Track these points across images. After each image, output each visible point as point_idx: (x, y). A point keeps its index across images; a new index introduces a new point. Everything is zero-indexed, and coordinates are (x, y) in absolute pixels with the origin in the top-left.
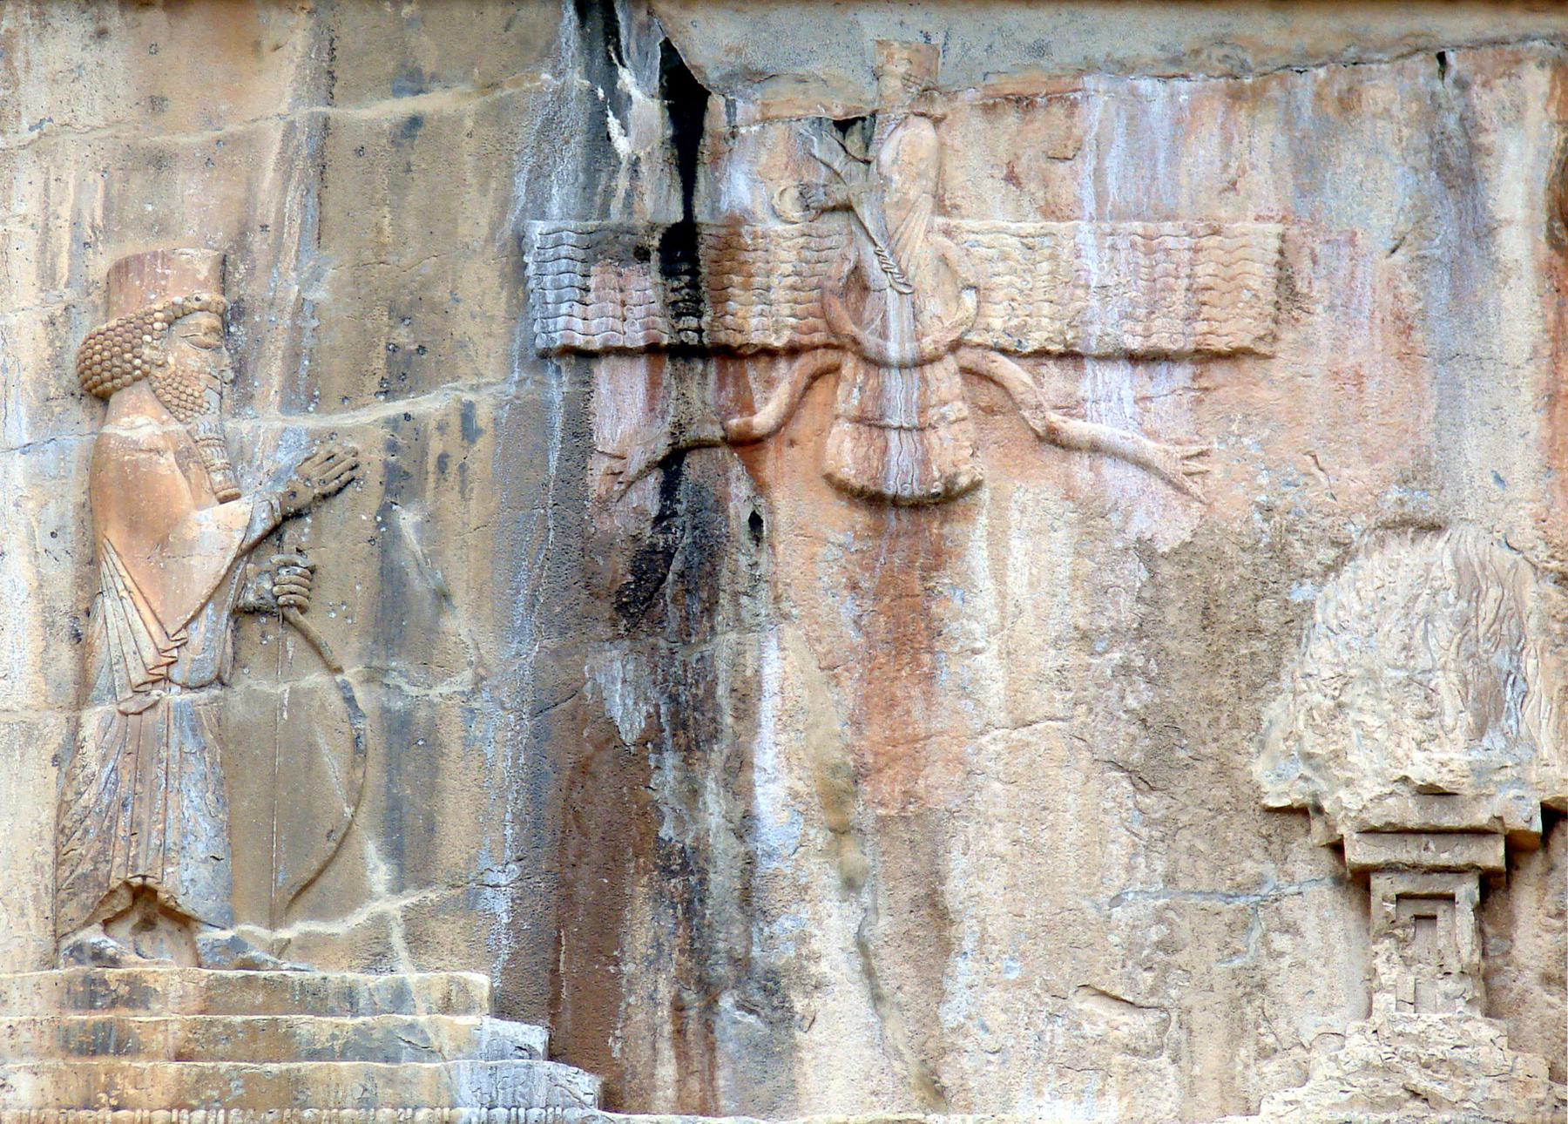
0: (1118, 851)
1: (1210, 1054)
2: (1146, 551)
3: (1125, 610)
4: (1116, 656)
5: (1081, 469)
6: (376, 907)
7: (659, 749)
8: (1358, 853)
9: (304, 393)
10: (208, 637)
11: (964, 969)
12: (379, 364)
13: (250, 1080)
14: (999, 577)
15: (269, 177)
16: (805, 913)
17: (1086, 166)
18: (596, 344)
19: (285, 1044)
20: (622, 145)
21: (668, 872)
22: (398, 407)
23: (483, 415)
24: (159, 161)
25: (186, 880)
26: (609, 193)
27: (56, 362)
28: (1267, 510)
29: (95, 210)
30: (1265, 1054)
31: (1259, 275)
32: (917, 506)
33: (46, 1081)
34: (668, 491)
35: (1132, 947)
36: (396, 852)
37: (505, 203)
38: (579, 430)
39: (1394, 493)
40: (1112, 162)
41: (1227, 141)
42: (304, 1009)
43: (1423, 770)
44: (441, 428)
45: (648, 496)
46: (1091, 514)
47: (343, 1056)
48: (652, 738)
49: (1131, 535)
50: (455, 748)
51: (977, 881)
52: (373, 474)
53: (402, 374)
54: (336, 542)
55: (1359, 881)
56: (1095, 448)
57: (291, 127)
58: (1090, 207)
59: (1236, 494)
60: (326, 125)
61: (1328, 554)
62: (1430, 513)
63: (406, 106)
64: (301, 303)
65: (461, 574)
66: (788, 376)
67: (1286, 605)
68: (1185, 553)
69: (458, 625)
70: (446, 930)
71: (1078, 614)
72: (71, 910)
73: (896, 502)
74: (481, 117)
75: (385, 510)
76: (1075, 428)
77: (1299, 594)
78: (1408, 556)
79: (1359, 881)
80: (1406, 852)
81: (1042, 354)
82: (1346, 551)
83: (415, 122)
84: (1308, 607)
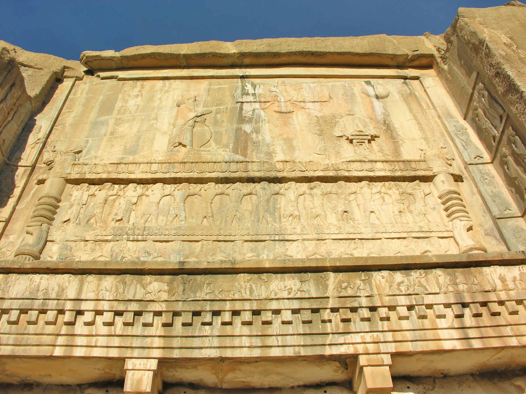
0: (317, 141)
2: (317, 117)
3: (315, 121)
5: (307, 110)
8: (350, 137)
9: (205, 105)
10: (191, 122)
11: (297, 152)
12: (215, 104)
14: (297, 118)
16: (274, 147)
23: (229, 108)
27: (174, 104)
31: (327, 96)
32: (286, 113)
34: (253, 113)
35: (320, 150)
37: (232, 93)
38: (241, 109)
40: (307, 89)
43: (358, 130)
45: (251, 113)
46: (309, 114)
48: (252, 132)
52: (214, 112)
55: (351, 142)
62: (352, 113)
63: (220, 86)
66: (268, 104)
69: (225, 124)
71: (308, 121)
72: (170, 145)
73: (283, 113)
76: (306, 107)
77: (337, 120)
83: (220, 88)
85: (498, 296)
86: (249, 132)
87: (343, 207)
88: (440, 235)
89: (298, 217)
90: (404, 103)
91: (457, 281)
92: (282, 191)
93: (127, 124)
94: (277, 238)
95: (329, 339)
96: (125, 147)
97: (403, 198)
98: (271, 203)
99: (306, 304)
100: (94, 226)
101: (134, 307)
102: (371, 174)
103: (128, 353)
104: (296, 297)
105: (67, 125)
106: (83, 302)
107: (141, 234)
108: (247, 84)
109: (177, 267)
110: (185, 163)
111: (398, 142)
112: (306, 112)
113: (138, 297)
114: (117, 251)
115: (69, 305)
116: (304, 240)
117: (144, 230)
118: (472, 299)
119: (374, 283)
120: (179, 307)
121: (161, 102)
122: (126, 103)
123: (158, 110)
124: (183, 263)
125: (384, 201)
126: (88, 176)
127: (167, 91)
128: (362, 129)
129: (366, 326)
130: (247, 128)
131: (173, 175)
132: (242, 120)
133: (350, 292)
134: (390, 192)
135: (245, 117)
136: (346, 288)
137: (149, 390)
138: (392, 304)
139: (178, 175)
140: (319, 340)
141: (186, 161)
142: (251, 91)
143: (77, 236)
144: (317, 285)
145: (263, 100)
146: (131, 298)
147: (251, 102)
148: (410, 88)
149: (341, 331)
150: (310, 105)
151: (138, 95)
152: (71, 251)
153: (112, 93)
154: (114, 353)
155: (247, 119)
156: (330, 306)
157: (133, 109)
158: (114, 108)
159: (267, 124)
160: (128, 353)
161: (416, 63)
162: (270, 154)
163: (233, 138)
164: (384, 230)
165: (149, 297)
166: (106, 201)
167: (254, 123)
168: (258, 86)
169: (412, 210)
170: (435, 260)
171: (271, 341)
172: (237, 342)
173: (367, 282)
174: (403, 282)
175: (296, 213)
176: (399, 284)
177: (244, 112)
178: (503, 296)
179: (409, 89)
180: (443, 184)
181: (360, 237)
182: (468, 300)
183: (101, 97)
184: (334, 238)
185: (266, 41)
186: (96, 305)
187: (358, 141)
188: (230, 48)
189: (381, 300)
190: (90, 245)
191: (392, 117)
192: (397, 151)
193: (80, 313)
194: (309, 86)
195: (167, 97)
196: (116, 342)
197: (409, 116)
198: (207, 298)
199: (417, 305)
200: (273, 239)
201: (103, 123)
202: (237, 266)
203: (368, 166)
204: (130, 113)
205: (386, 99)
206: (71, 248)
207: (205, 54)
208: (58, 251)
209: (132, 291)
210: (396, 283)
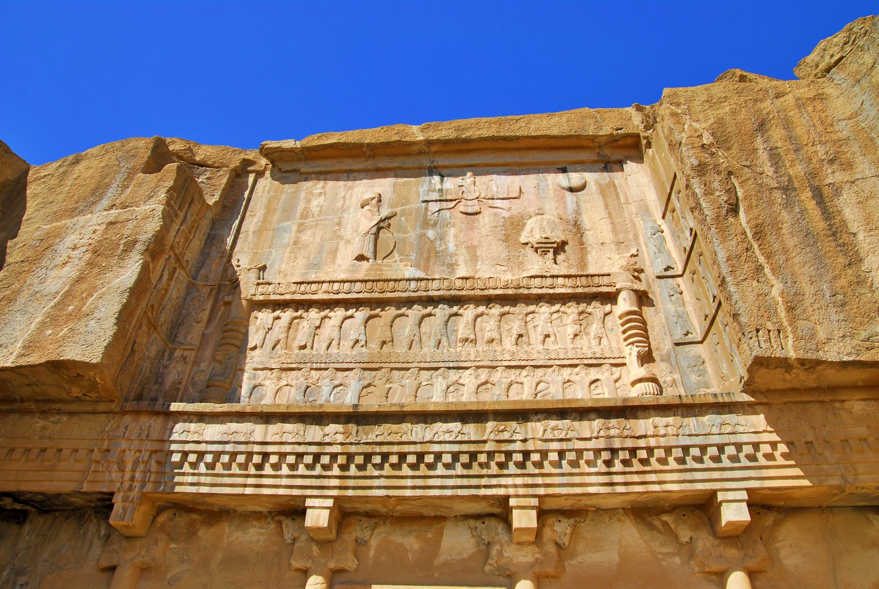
1: (516, 271)
2: (504, 218)
3: (501, 223)
8: (536, 246)
9: (391, 206)
10: (374, 230)
11: (480, 262)
19: (381, 270)
25: (369, 254)
31: (518, 190)
38: (427, 209)
43: (544, 236)
53: (403, 205)
59: (515, 212)
66: (454, 203)
68: (509, 218)
69: (409, 228)
71: (495, 224)
78: (539, 217)
88: (613, 361)
92: (460, 312)
97: (581, 317)
99: (465, 448)
101: (314, 449)
103: (308, 492)
105: (250, 233)
109: (351, 410)
113: (317, 440)
118: (622, 444)
120: (353, 449)
121: (345, 201)
126: (273, 297)
128: (548, 235)
133: (506, 436)
134: (569, 311)
136: (502, 431)
137: (326, 525)
140: (474, 482)
150: (498, 203)
154: (295, 492)
156: (486, 449)
160: (308, 492)
162: (452, 267)
164: (557, 357)
165: (327, 439)
166: (291, 324)
172: (403, 482)
175: (472, 337)
177: (429, 213)
185: (455, 123)
188: (416, 133)
189: (534, 444)
190: (276, 373)
192: (583, 262)
193: (266, 456)
197: (603, 213)
198: (378, 439)
201: (285, 230)
202: (405, 409)
203: (549, 281)
204: (313, 216)
207: (390, 142)
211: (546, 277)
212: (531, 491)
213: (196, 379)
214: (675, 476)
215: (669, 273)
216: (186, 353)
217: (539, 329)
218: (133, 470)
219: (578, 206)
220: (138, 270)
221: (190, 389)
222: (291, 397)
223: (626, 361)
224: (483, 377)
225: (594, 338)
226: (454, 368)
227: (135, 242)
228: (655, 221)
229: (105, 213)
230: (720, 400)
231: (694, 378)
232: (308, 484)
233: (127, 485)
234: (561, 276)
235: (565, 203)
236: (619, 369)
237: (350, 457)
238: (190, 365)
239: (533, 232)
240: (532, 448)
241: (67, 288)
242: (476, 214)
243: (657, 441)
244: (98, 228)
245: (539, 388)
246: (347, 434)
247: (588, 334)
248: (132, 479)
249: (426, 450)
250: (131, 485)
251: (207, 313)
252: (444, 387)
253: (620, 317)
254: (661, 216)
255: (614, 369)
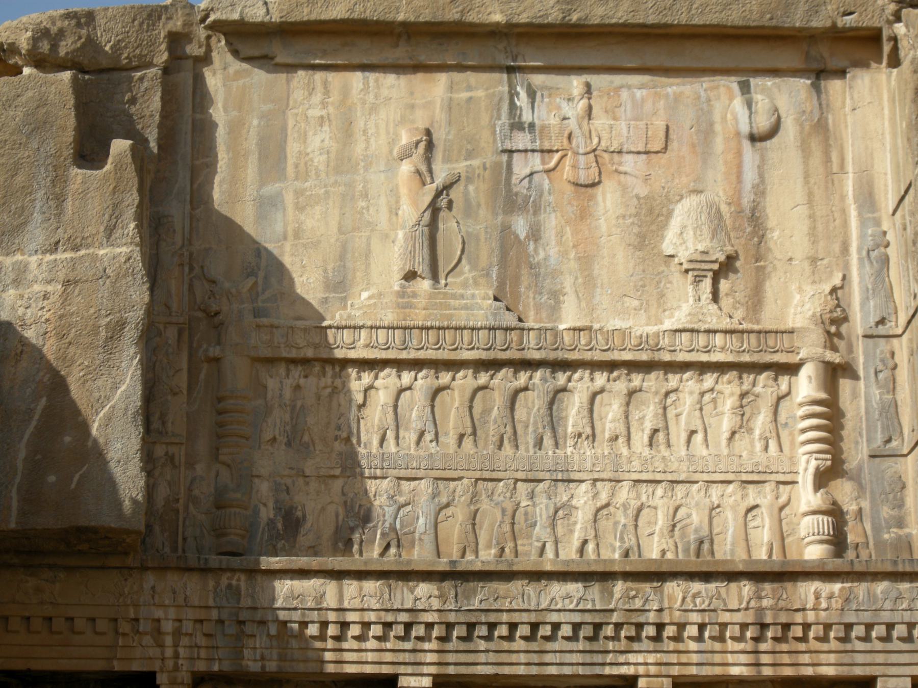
1: (653, 311)
2: (638, 197)
3: (633, 211)
4: (631, 220)
5: (622, 177)
6: (466, 275)
7: (529, 240)
12: (464, 152)
13: (441, 315)
14: (604, 201)
15: (438, 111)
17: (623, 109)
18: (514, 149)
19: (448, 307)
20: (518, 104)
21: (531, 268)
22: (468, 163)
23: (488, 166)
24: (412, 107)
26: (515, 115)
28: (664, 188)
29: (398, 118)
30: (664, 311)
31: (662, 134)
32: (586, 186)
33: (395, 315)
34: (530, 182)
35: (635, 286)
36: (470, 263)
37: (492, 117)
39: (692, 184)
41: (654, 104)
42: (451, 298)
43: (701, 247)
44: (479, 168)
46: (624, 188)
47: (462, 309)
48: (527, 237)
49: (634, 193)
50: (483, 240)
51: (600, 270)
53: (469, 155)
54: (456, 194)
56: (625, 173)
57: (442, 100)
58: (623, 118)
60: (451, 98)
61: (677, 198)
62: (701, 188)
63: (469, 94)
64: (445, 140)
65: (483, 202)
66: (557, 157)
67: (668, 209)
68: (647, 198)
69: (482, 212)
70: (482, 281)
71: (621, 211)
74: (486, 96)
75: (466, 186)
76: (621, 169)
79: (687, 271)
80: (698, 266)
81: (613, 152)
82: (682, 197)
83: (471, 98)
84: (673, 210)
85: (805, 617)
86: (522, 236)
87: (655, 422)
89: (591, 438)
90: (800, 152)
91: (763, 594)
93: (318, 208)
94: (560, 477)
95: (610, 658)
96: (325, 271)
98: (555, 407)
100: (312, 448)
101: (404, 617)
102: (704, 358)
103: (402, 669)
104: (579, 608)
106: (347, 613)
107: (379, 466)
108: (519, 89)
109: (448, 569)
110: (428, 329)
111: (764, 268)
112: (619, 183)
113: (408, 605)
114: (351, 495)
115: (332, 616)
116: (595, 480)
117: (383, 460)
119: (666, 592)
120: (452, 618)
121: (367, 141)
122: (305, 142)
123: (366, 170)
124: (453, 563)
125: (715, 408)
126: (285, 354)
127: (374, 109)
129: (651, 646)
130: (520, 226)
131: (412, 355)
132: (510, 201)
133: (638, 604)
135: (516, 194)
136: (634, 597)
138: (682, 621)
139: (422, 355)
140: (598, 658)
141: (429, 324)
142: (527, 117)
143: (292, 469)
144: (602, 592)
145: (547, 146)
146: (400, 607)
147: (526, 151)
148: (824, 102)
149: (623, 649)
150: (629, 163)
151: (322, 117)
152: (288, 493)
153: (270, 106)
154: (386, 670)
155: (520, 201)
156: (614, 620)
157: (319, 160)
158: (286, 157)
159: (553, 215)
160: (402, 669)
161: (850, 34)
162: (556, 296)
163: (497, 252)
167: (531, 212)
168: (539, 94)
169: (752, 426)
170: (741, 568)
171: (548, 658)
172: (514, 658)
173: (659, 591)
174: (699, 593)
176: (694, 596)
178: (811, 617)
179: (820, 104)
180: (806, 385)
181: (670, 479)
182: (768, 619)
183: (255, 122)
184: (636, 478)
186: (362, 616)
187: (696, 273)
189: (671, 615)
190: (314, 485)
191: (768, 199)
192: (755, 301)
193: (345, 625)
194: (633, 97)
195: (377, 126)
196: (388, 657)
197: (800, 195)
198: (483, 607)
199: (710, 624)
200: (554, 478)
202: (515, 568)
203: (702, 340)
204: (317, 175)
205: (768, 142)
206: (288, 488)
208: (271, 494)
209: (399, 596)
210: (690, 594)
211: (698, 331)
212: (664, 670)
213: (196, 492)
214: (832, 658)
215: (882, 330)
216: (173, 450)
217: (683, 418)
218: (176, 645)
219: (761, 176)
220: (139, 372)
221: (191, 507)
222: (340, 523)
223: (800, 479)
224: (604, 497)
225: (760, 439)
226: (563, 481)
227: (121, 324)
228: (877, 222)
229: (49, 257)
230: (900, 569)
231: (886, 512)
232: (401, 660)
233: (170, 664)
234: (721, 331)
235: (740, 166)
236: (789, 487)
237: (450, 626)
238: (183, 469)
239: (685, 235)
240: (667, 621)
241: (43, 401)
242: (593, 185)
243: (817, 615)
244: (50, 288)
245: (679, 516)
246: (442, 597)
247: (750, 431)
248: (176, 656)
249: (540, 619)
250: (176, 664)
251: (184, 375)
252: (551, 511)
253: (801, 405)
254: (891, 211)
255: (781, 487)
